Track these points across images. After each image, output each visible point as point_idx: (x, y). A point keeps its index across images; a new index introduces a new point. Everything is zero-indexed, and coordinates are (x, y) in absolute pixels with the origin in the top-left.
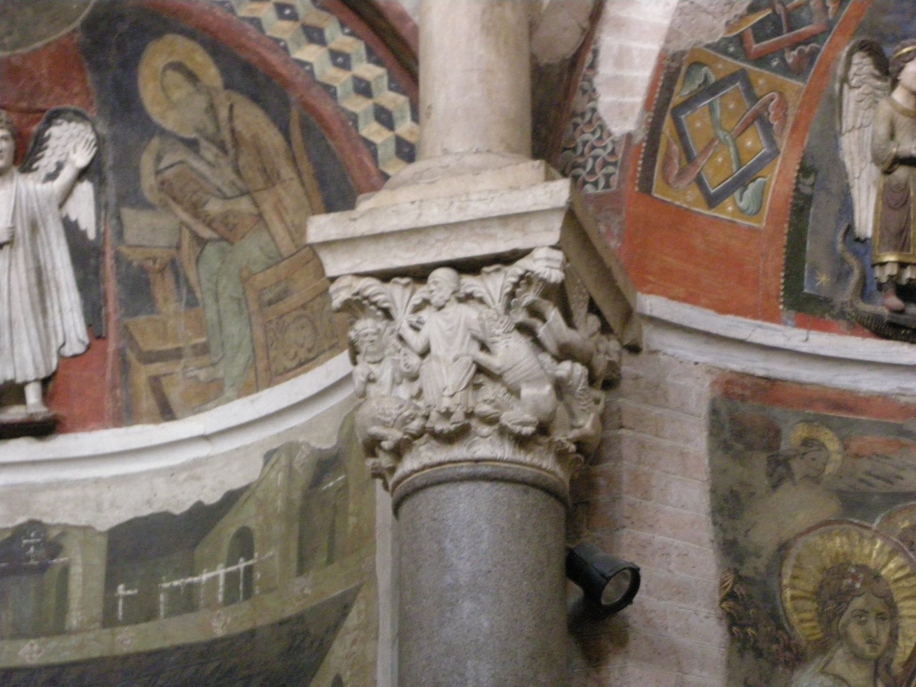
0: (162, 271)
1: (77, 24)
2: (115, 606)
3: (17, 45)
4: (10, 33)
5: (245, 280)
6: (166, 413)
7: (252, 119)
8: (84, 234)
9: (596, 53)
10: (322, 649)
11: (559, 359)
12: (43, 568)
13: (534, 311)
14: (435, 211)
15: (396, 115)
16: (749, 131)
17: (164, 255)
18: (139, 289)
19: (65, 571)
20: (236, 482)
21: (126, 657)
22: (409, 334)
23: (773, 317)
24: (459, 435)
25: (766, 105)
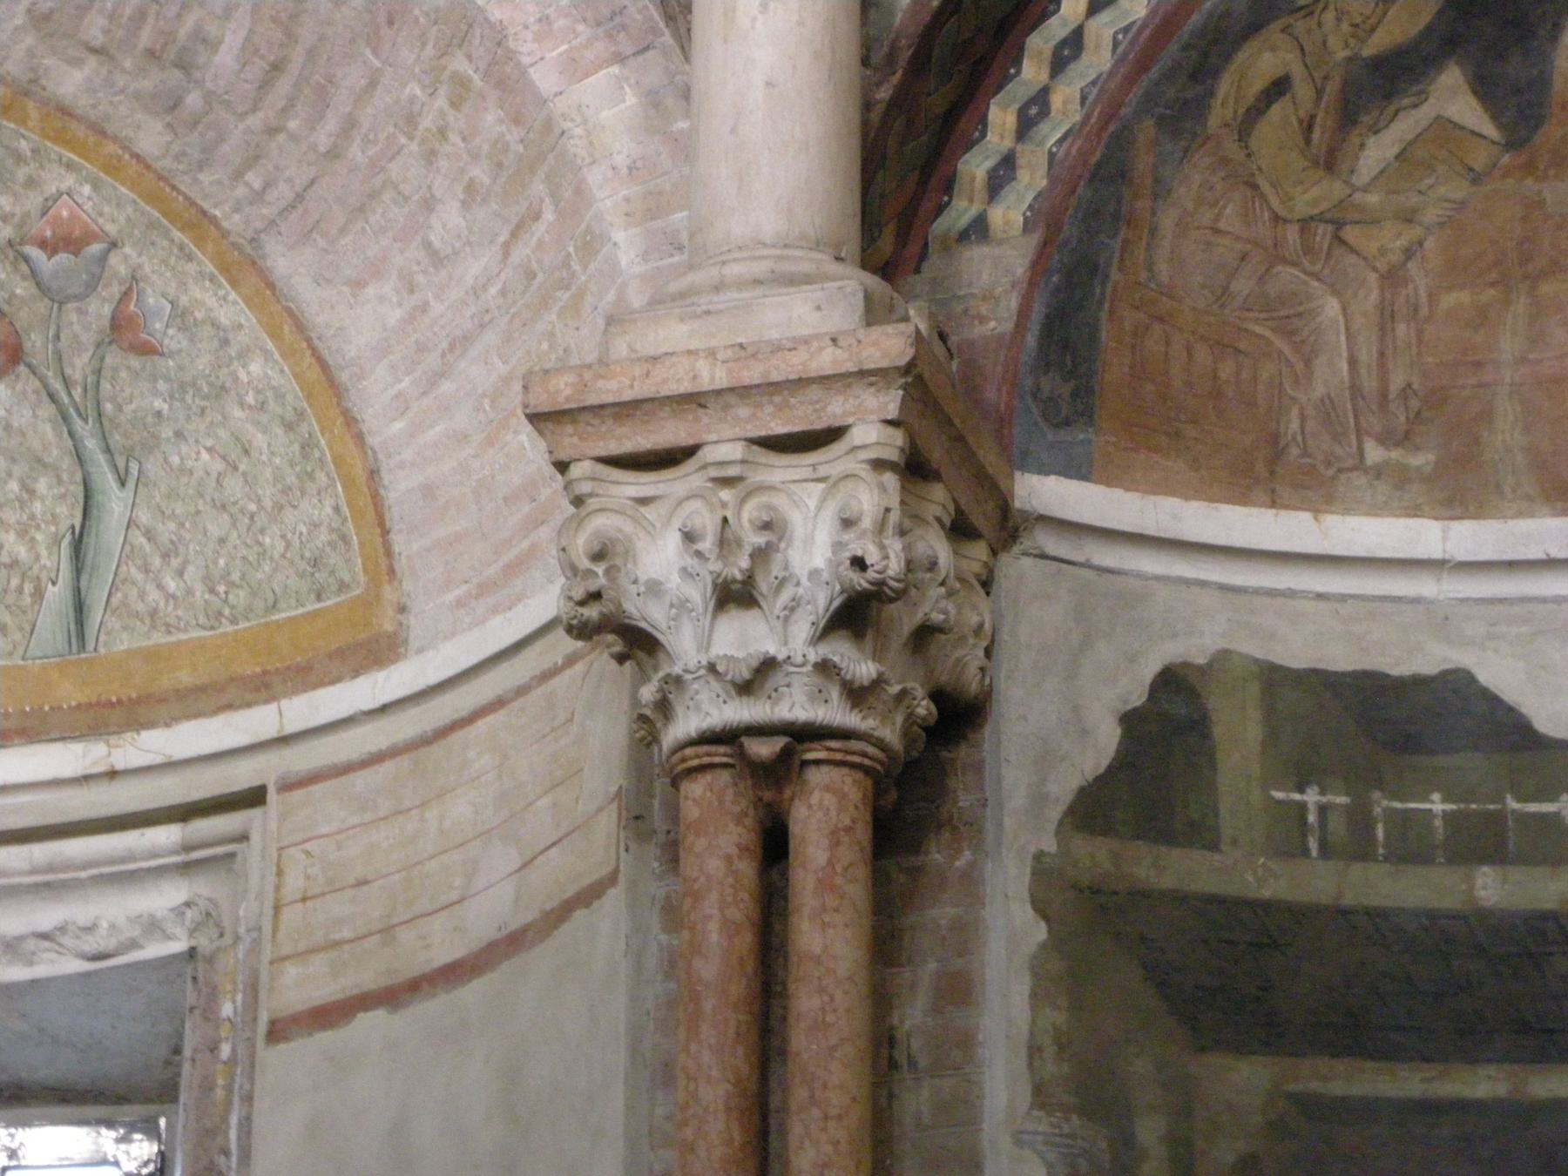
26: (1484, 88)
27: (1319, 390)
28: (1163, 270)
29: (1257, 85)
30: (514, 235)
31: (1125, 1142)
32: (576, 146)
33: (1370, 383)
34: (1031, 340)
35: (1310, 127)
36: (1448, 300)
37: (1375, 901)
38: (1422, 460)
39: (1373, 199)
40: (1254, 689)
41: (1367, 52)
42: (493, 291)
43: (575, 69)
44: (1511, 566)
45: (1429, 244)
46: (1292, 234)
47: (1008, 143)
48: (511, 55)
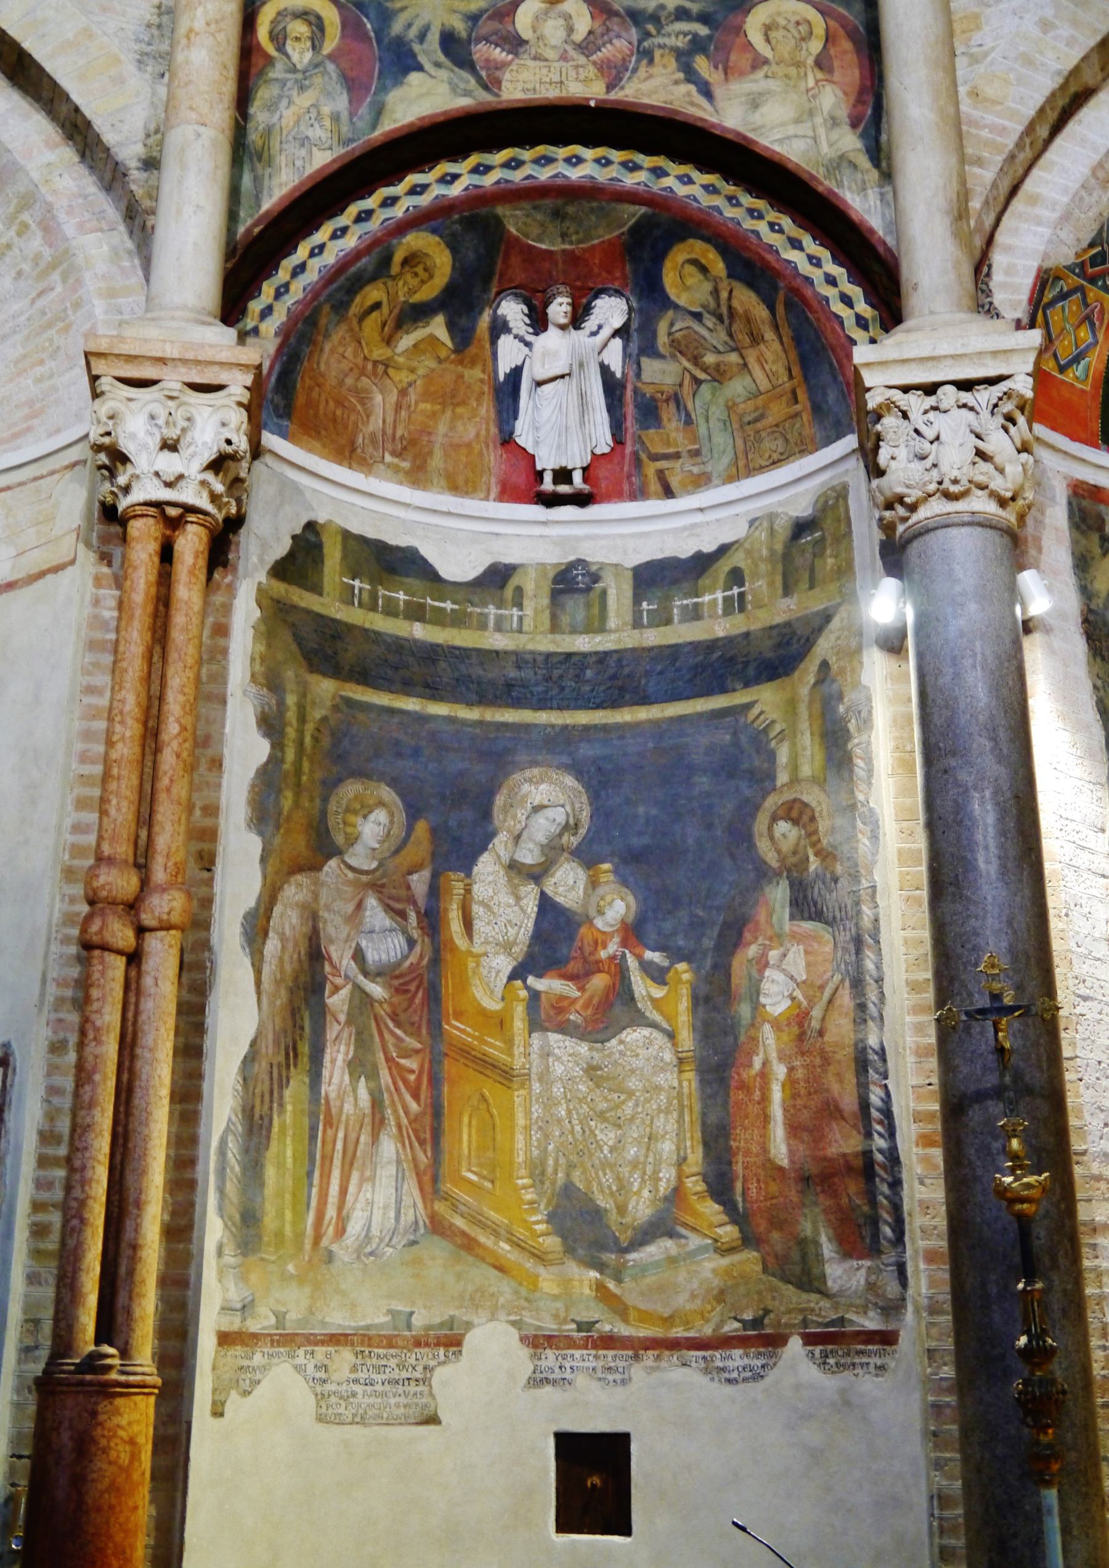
0: (667, 401)
1: (625, 229)
2: (641, 617)
3: (580, 242)
4: (577, 233)
5: (730, 407)
6: (668, 493)
7: (746, 299)
8: (613, 374)
9: (990, 267)
10: (808, 644)
11: (1019, 452)
12: (588, 589)
13: (1010, 419)
14: (945, 346)
15: (854, 299)
16: (1083, 327)
17: (670, 390)
18: (649, 412)
19: (604, 593)
20: (727, 539)
21: (651, 649)
22: (923, 429)
23: (1097, 447)
24: (964, 494)
25: (1093, 311)
26: (451, 326)
27: (371, 428)
28: (323, 367)
29: (369, 302)
30: (40, 295)
31: (281, 703)
32: (80, 260)
33: (389, 431)
34: (273, 379)
35: (384, 325)
36: (422, 406)
37: (376, 628)
38: (406, 465)
39: (401, 360)
40: (339, 538)
41: (411, 301)
42: (23, 318)
43: (81, 228)
44: (435, 511)
45: (419, 382)
46: (370, 366)
47: (270, 300)
48: (54, 218)
